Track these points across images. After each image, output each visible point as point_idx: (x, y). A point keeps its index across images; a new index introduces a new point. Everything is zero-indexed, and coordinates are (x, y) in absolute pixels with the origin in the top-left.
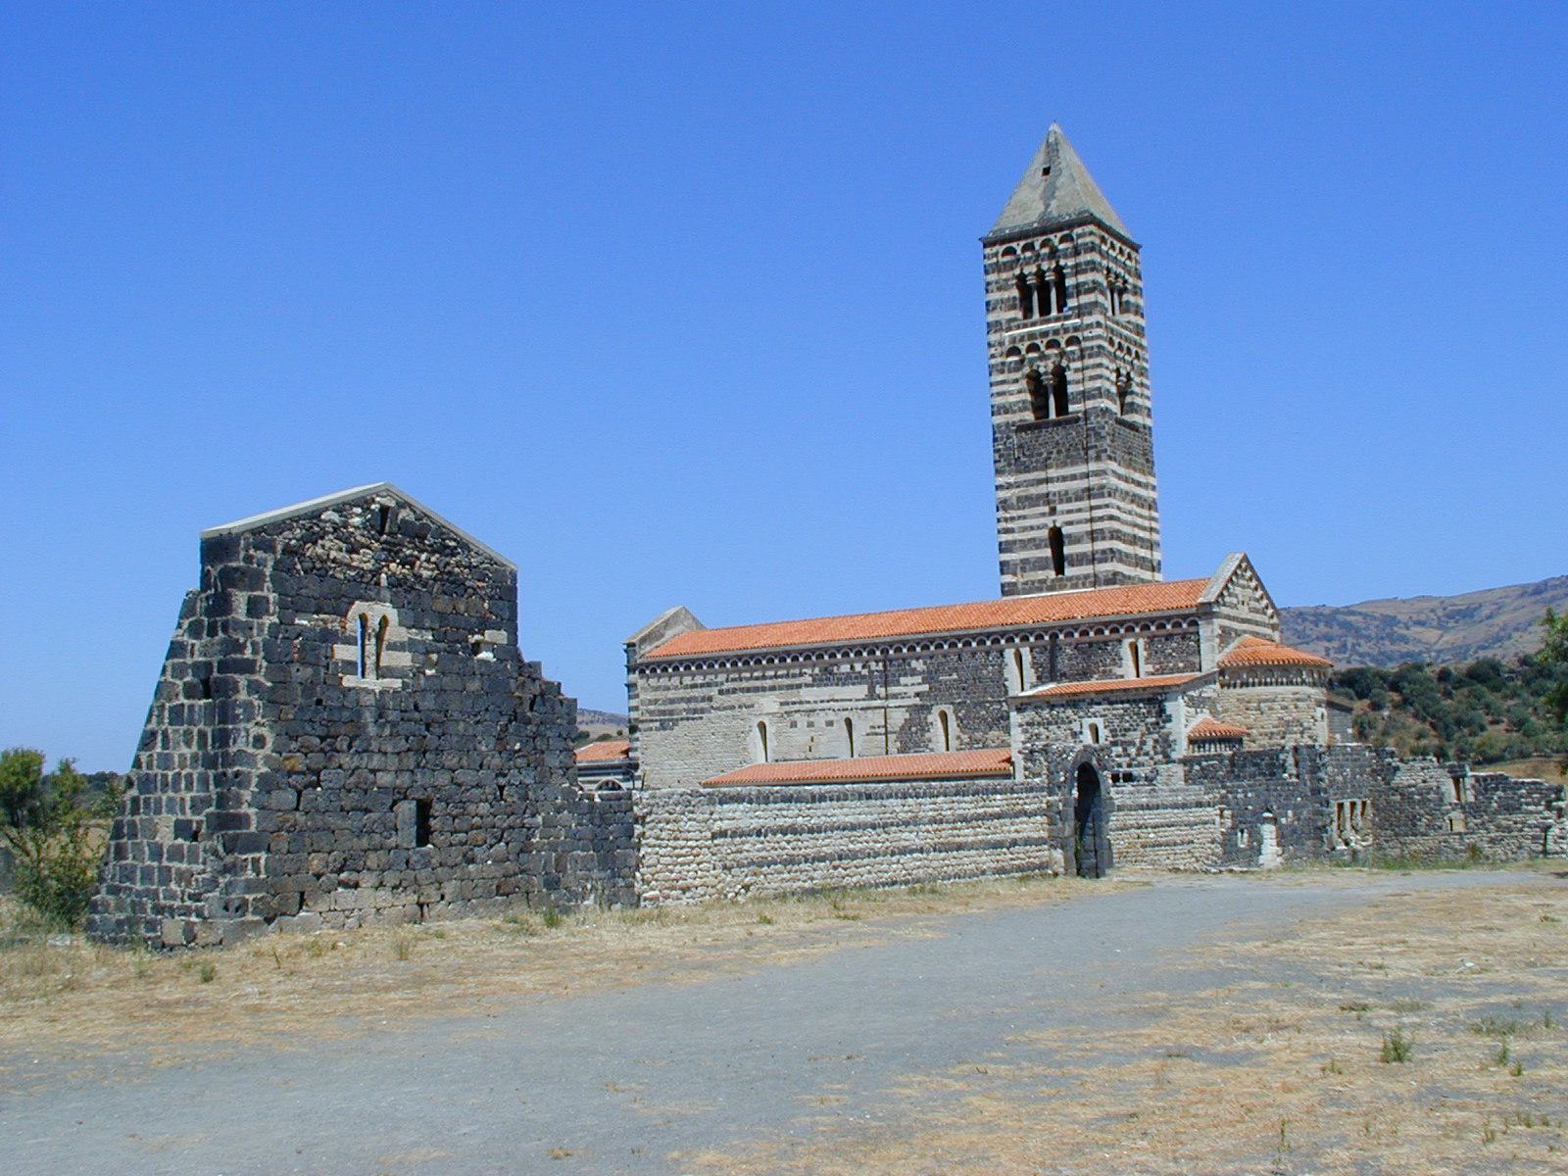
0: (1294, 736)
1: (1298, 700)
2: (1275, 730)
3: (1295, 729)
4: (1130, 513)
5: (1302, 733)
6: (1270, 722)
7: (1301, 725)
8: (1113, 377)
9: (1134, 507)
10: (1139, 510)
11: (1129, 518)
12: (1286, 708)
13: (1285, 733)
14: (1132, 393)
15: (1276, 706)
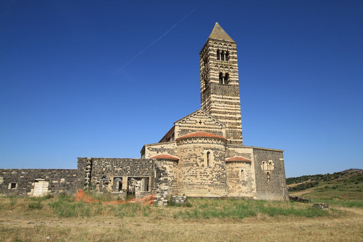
0: (193, 159)
1: (195, 148)
2: (187, 157)
3: (194, 157)
4: (224, 106)
5: (196, 158)
6: (186, 155)
7: (196, 155)
8: (218, 75)
9: (226, 105)
10: (229, 105)
11: (224, 108)
12: (191, 150)
13: (190, 158)
14: (230, 77)
15: (188, 150)
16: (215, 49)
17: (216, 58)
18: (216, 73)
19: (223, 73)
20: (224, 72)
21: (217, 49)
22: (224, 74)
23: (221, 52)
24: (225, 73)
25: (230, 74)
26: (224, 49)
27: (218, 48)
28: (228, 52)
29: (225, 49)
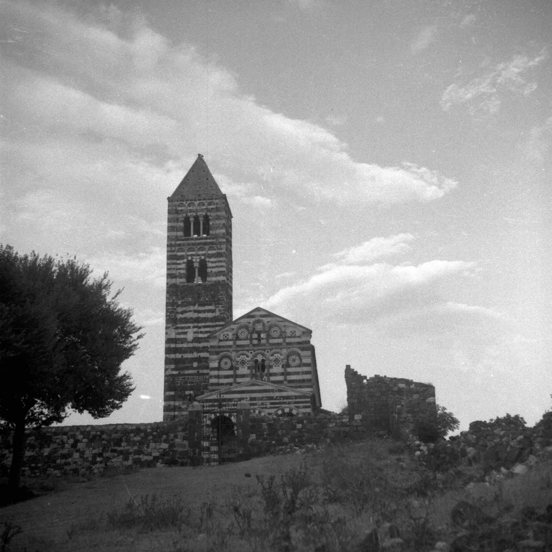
8: (183, 266)
16: (180, 216)
17: (181, 234)
18: (180, 264)
19: (194, 260)
20: (196, 260)
21: (184, 215)
22: (196, 262)
23: (192, 219)
24: (198, 260)
25: (209, 262)
26: (199, 214)
27: (186, 214)
28: (206, 218)
29: (201, 213)
